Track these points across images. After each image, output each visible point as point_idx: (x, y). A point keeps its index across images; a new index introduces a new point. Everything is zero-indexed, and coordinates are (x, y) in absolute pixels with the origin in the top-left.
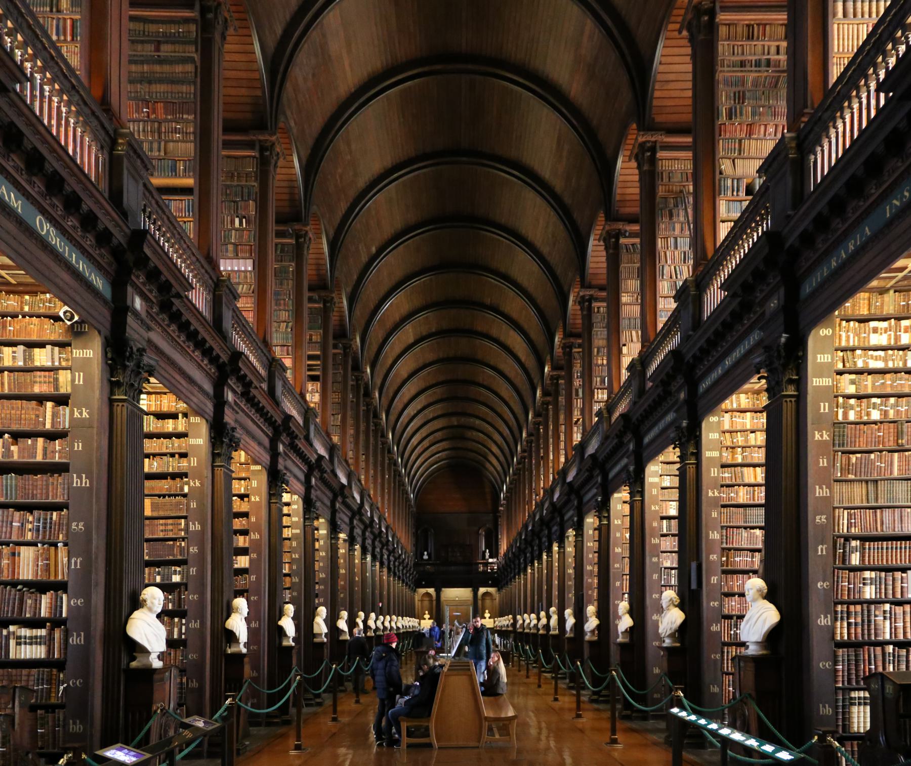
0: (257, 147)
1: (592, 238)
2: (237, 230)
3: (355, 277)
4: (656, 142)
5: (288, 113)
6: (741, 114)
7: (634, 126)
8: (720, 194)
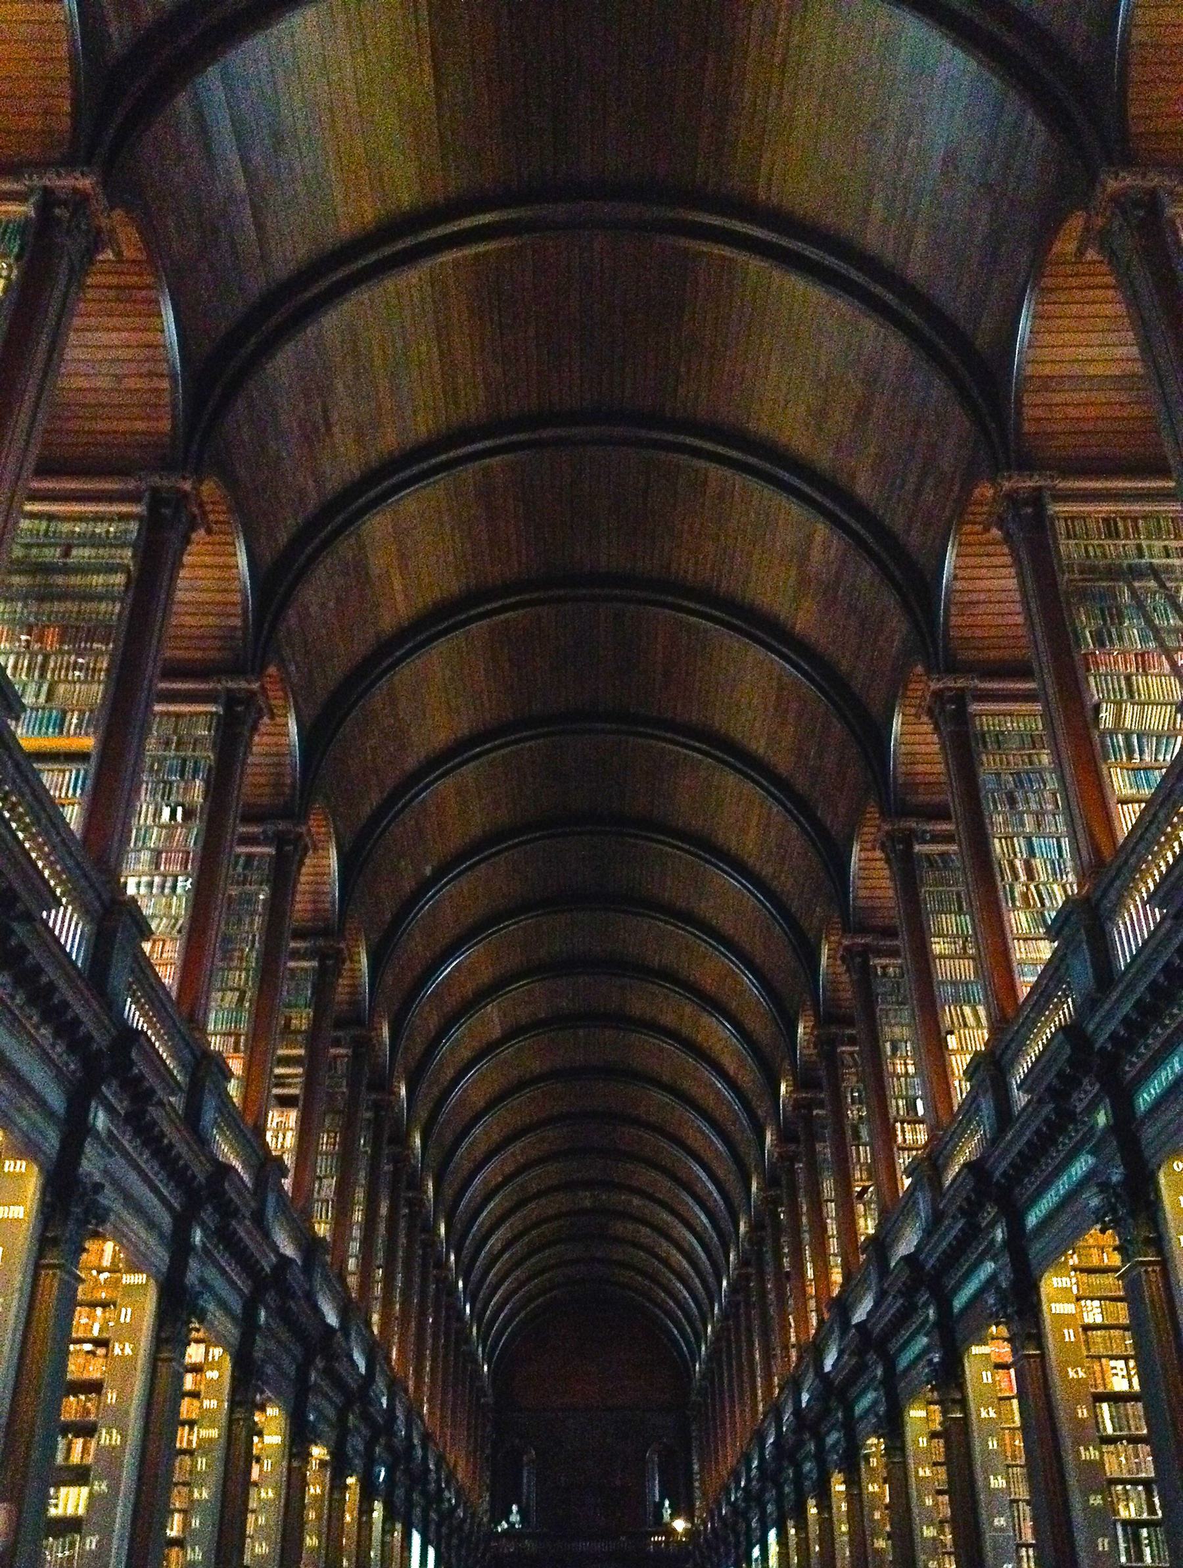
0: (223, 699)
1: (856, 848)
2: (162, 827)
3: (388, 916)
4: (962, 689)
5: (287, 652)
6: (1121, 638)
7: (919, 669)
8: (1106, 758)
